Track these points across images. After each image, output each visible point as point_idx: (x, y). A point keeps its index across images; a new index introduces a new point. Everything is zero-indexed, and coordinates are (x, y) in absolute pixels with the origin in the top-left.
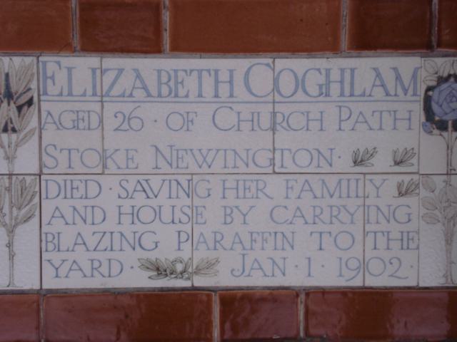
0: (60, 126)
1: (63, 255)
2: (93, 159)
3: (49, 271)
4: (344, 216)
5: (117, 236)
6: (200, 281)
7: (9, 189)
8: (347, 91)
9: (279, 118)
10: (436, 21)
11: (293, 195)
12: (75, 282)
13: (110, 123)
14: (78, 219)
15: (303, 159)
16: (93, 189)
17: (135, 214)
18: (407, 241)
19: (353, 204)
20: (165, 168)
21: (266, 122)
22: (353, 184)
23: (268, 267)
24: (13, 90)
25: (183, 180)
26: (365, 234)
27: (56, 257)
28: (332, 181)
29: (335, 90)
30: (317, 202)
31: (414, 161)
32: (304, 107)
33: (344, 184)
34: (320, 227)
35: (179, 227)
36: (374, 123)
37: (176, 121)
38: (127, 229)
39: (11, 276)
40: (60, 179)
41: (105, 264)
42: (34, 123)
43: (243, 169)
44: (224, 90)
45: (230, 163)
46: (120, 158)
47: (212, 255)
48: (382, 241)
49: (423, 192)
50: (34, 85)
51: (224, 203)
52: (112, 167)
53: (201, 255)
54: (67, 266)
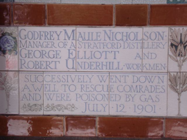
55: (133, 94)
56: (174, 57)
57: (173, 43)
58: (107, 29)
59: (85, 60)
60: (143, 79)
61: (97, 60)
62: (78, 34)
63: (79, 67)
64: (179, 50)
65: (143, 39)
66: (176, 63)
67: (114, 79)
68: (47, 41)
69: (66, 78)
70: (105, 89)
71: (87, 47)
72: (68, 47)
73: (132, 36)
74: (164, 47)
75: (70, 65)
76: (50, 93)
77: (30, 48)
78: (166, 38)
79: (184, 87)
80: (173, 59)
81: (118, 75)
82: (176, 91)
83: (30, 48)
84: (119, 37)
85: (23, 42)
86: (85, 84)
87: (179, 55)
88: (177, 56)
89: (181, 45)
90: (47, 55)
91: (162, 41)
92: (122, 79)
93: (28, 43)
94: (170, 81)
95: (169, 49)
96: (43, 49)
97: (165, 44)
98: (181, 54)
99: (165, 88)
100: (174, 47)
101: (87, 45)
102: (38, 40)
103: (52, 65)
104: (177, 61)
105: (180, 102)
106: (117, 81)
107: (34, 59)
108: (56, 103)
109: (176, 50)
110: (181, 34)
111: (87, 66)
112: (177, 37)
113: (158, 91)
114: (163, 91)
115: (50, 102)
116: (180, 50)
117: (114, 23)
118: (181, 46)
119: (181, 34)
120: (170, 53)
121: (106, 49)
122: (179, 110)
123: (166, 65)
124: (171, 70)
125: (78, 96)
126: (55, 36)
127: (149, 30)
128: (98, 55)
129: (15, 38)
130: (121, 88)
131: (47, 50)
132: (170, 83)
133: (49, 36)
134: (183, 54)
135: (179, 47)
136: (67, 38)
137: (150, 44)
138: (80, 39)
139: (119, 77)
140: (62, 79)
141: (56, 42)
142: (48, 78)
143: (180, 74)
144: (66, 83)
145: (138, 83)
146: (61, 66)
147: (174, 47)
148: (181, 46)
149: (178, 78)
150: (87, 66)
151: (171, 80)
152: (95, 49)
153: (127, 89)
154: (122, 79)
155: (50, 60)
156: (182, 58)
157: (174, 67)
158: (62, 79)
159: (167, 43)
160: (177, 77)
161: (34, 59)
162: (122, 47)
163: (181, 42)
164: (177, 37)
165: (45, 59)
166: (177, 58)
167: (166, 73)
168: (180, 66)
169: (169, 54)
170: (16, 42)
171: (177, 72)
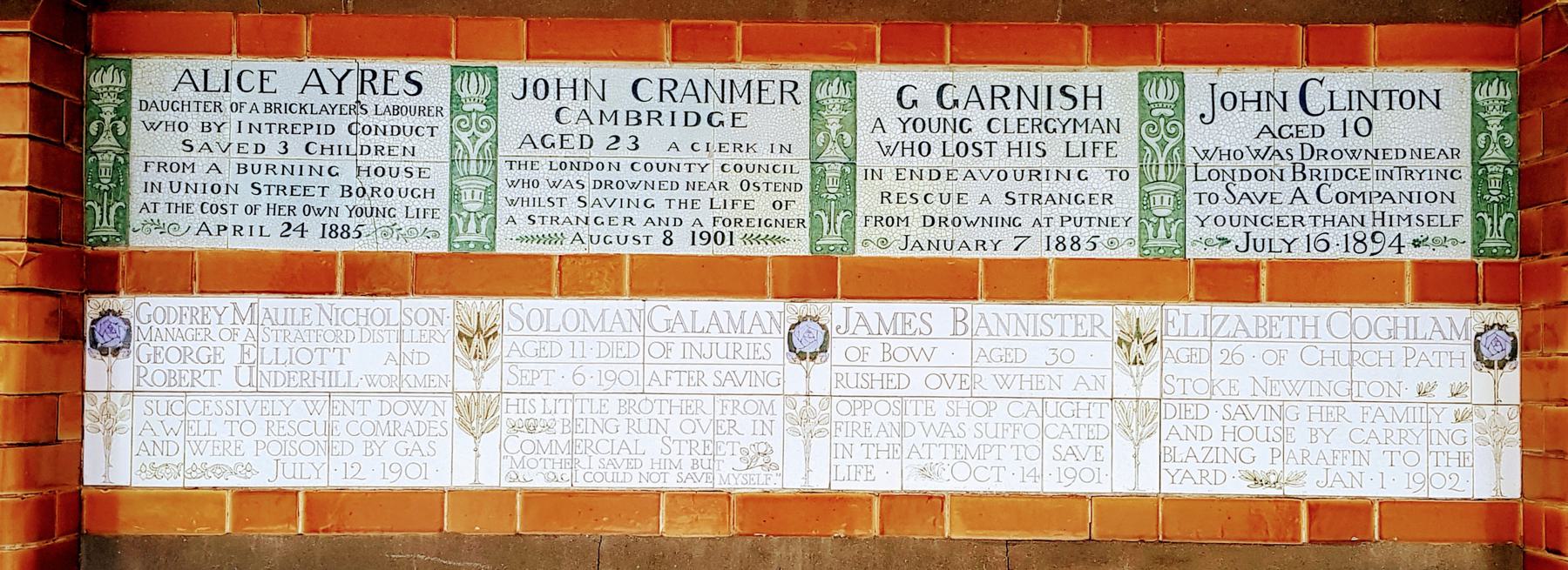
0: (1177, 360)
1: (1178, 466)
2: (1202, 387)
3: (1166, 477)
4: (1411, 438)
5: (1221, 451)
6: (1290, 491)
7: (1136, 410)
8: (1412, 335)
9: (1356, 356)
10: (1481, 282)
11: (1368, 419)
12: (1188, 489)
13: (1218, 358)
14: (1190, 436)
15: (1376, 390)
16: (1202, 412)
17: (1236, 432)
18: (1462, 460)
19: (1418, 428)
20: (1261, 395)
21: (1345, 359)
22: (1418, 411)
23: (1347, 480)
24: (1142, 330)
25: (1276, 405)
26: (1429, 453)
27: (1172, 467)
28: (1400, 409)
29: (1401, 333)
30: (1387, 426)
31: (1468, 393)
32: (1377, 348)
33: (1411, 410)
34: (1391, 447)
35: (1273, 445)
36: (1434, 360)
37: (1270, 357)
38: (1230, 445)
39: (1136, 483)
40: (1176, 403)
41: (1212, 474)
42: (1157, 358)
43: (1326, 397)
44: (1310, 332)
45: (1315, 393)
46: (1224, 386)
47: (1300, 469)
48: (1442, 459)
49: (1476, 420)
50: (1158, 328)
51: (1310, 425)
52: (1218, 395)
53: (1291, 469)
54: (1181, 473)
55: (379, 441)
58: (324, 301)
59: (277, 368)
60: (401, 408)
61: (304, 368)
62: (262, 312)
63: (265, 384)
65: (401, 324)
67: (340, 409)
68: (195, 326)
69: (234, 406)
70: (321, 430)
71: (281, 339)
72: (240, 340)
73: (378, 318)
75: (244, 380)
76: (198, 438)
77: (159, 343)
78: (448, 322)
81: (348, 400)
83: (159, 343)
84: (350, 317)
85: (144, 329)
86: (275, 419)
90: (194, 356)
91: (439, 327)
92: (358, 408)
93: (154, 331)
96: (186, 343)
99: (448, 426)
101: (281, 334)
102: (176, 326)
103: (206, 379)
106: (347, 412)
107: (166, 366)
108: (211, 462)
111: (280, 380)
113: (433, 432)
115: (199, 460)
117: (339, 288)
120: (458, 353)
121: (322, 344)
124: (458, 387)
125: (261, 445)
126: (213, 315)
127: (412, 303)
128: (304, 356)
129: (127, 322)
130: (354, 429)
131: (195, 346)
132: (457, 416)
133: (199, 317)
135: (475, 341)
136: (238, 321)
137: (416, 335)
138: (268, 323)
139: (350, 404)
140: (226, 409)
141: (215, 329)
142: (195, 408)
144: (234, 418)
145: (392, 416)
146: (226, 381)
150: (280, 380)
152: (299, 344)
153: (368, 428)
154: (358, 411)
155: (201, 367)
156: (482, 363)
157: (465, 381)
158: (226, 409)
161: (166, 366)
162: (358, 338)
165: (190, 365)
170: (129, 331)
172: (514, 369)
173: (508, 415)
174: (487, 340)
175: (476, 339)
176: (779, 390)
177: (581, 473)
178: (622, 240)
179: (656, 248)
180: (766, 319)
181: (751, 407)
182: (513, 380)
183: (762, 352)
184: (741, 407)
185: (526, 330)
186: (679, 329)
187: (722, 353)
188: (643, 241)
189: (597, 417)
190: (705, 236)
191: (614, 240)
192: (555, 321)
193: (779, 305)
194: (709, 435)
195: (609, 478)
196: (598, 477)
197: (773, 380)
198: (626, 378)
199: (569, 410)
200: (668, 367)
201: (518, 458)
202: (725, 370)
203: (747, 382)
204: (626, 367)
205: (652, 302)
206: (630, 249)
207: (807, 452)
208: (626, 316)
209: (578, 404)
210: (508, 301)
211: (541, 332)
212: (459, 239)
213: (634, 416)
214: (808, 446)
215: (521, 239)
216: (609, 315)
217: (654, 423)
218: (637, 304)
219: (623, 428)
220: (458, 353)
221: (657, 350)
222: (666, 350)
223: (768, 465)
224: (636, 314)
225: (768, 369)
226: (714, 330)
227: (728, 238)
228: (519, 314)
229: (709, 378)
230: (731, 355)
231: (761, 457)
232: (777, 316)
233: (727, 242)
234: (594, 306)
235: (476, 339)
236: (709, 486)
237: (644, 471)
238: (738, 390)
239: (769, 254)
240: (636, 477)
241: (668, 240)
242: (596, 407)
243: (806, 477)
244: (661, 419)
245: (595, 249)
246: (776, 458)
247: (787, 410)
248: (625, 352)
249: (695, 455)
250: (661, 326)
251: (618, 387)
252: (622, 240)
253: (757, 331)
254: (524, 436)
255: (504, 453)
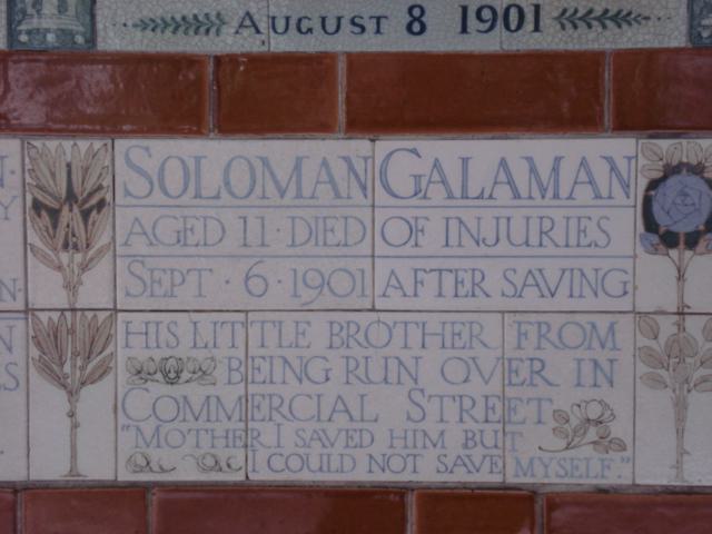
56: (50, 253)
57: (40, 198)
64: (65, 224)
66: (58, 277)
74: (6, 214)
78: (13, 181)
79: (90, 367)
80: (45, 259)
82: (60, 381)
87: (66, 246)
88: (60, 246)
89: (71, 206)
94: (38, 344)
95: (29, 224)
97: (12, 201)
98: (72, 240)
99: (19, 372)
100: (44, 213)
104: (60, 268)
105: (75, 426)
109: (55, 226)
110: (69, 165)
112: (53, 175)
114: (12, 384)
116: (68, 226)
118: (71, 210)
119: (69, 165)
120: (33, 238)
122: (74, 456)
123: (20, 284)
124: (37, 300)
132: (35, 352)
134: (82, 242)
135: (65, 215)
143: (74, 317)
147: (44, 213)
148: (71, 210)
149: (64, 333)
151: (40, 338)
156: (78, 257)
157: (48, 290)
159: (19, 201)
160: (64, 329)
163: (71, 196)
164: (53, 175)
166: (58, 259)
167: (22, 315)
168: (72, 287)
169: (29, 241)
171: (63, 310)
172: (137, 268)
173: (127, 349)
174: (86, 215)
175: (67, 215)
176: (625, 304)
177: (262, 455)
178: (331, 27)
179: (395, 40)
180: (601, 171)
181: (572, 335)
182: (136, 288)
183: (593, 233)
184: (553, 336)
185: (158, 197)
186: (437, 194)
187: (518, 237)
188: (371, 26)
189: (291, 354)
190: (486, 14)
191: (316, 25)
192: (212, 179)
193: (622, 147)
194: (495, 386)
195: (314, 463)
196: (295, 463)
197: (613, 284)
198: (341, 283)
199: (240, 341)
200: (420, 264)
201: (148, 428)
202: (523, 266)
203: (564, 290)
204: (342, 263)
205: (386, 145)
206: (345, 43)
207: (680, 419)
208: (339, 169)
209: (254, 331)
210: (122, 144)
211: (186, 199)
212: (23, 27)
213: (357, 352)
214: (681, 406)
215: (143, 25)
216: (310, 171)
217: (393, 365)
218: (359, 146)
219: (338, 373)
220: (33, 238)
221: (397, 231)
222: (414, 230)
223: (606, 443)
224: (359, 166)
225: (605, 265)
226: (503, 193)
227: (530, 17)
228: (145, 164)
229: (494, 282)
230: (534, 240)
231: (596, 428)
232: (622, 165)
233: (529, 26)
234: (280, 151)
235: (67, 215)
236: (496, 479)
237: (378, 449)
238: (545, 304)
239: (608, 46)
240: (363, 464)
241: (417, 22)
242: (289, 332)
243: (678, 465)
244: (406, 356)
245: (282, 44)
246: (618, 429)
247: (643, 341)
248: (340, 235)
249: (470, 425)
250: (403, 185)
251: (328, 301)
252: (331, 27)
253: (584, 194)
254: (158, 388)
255: (122, 420)
